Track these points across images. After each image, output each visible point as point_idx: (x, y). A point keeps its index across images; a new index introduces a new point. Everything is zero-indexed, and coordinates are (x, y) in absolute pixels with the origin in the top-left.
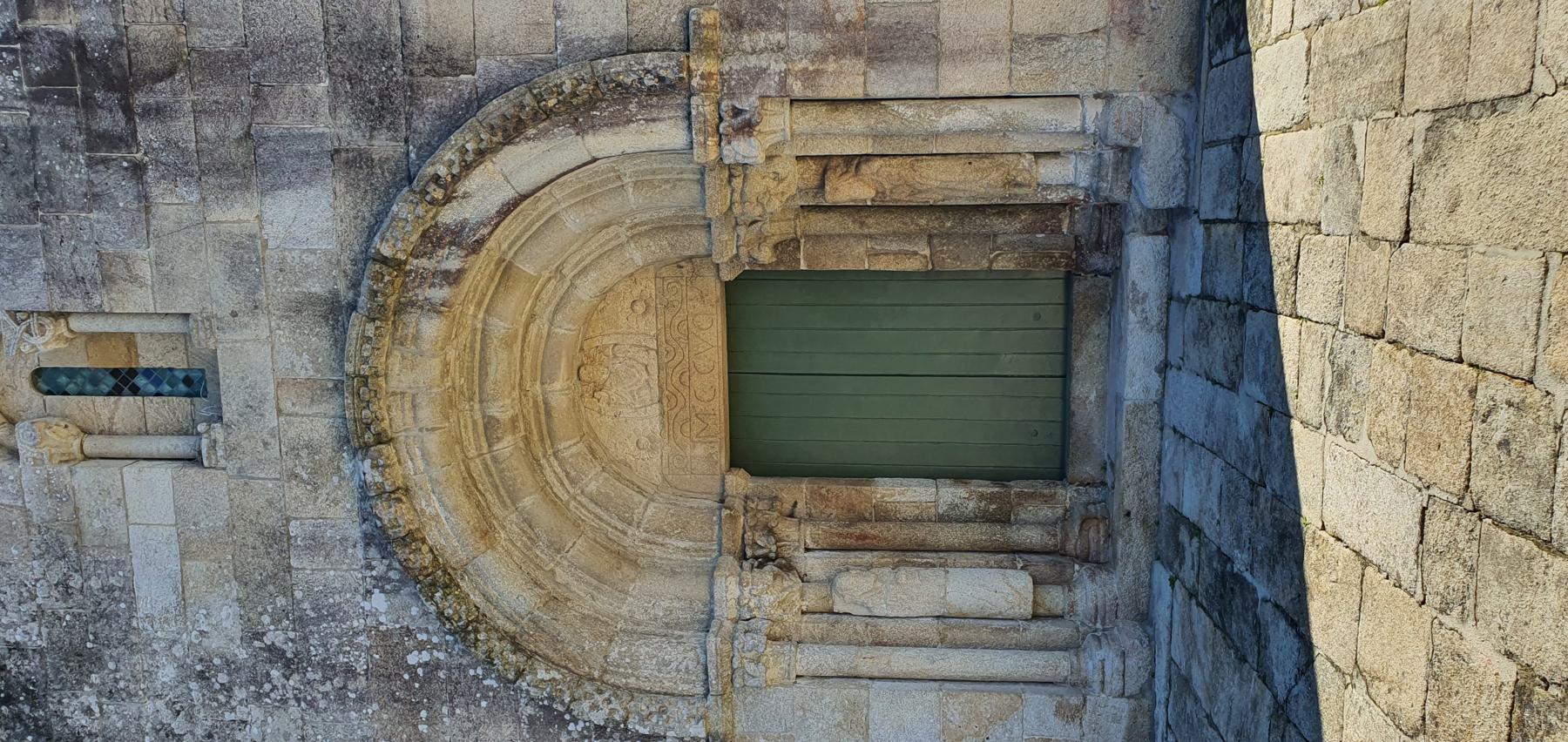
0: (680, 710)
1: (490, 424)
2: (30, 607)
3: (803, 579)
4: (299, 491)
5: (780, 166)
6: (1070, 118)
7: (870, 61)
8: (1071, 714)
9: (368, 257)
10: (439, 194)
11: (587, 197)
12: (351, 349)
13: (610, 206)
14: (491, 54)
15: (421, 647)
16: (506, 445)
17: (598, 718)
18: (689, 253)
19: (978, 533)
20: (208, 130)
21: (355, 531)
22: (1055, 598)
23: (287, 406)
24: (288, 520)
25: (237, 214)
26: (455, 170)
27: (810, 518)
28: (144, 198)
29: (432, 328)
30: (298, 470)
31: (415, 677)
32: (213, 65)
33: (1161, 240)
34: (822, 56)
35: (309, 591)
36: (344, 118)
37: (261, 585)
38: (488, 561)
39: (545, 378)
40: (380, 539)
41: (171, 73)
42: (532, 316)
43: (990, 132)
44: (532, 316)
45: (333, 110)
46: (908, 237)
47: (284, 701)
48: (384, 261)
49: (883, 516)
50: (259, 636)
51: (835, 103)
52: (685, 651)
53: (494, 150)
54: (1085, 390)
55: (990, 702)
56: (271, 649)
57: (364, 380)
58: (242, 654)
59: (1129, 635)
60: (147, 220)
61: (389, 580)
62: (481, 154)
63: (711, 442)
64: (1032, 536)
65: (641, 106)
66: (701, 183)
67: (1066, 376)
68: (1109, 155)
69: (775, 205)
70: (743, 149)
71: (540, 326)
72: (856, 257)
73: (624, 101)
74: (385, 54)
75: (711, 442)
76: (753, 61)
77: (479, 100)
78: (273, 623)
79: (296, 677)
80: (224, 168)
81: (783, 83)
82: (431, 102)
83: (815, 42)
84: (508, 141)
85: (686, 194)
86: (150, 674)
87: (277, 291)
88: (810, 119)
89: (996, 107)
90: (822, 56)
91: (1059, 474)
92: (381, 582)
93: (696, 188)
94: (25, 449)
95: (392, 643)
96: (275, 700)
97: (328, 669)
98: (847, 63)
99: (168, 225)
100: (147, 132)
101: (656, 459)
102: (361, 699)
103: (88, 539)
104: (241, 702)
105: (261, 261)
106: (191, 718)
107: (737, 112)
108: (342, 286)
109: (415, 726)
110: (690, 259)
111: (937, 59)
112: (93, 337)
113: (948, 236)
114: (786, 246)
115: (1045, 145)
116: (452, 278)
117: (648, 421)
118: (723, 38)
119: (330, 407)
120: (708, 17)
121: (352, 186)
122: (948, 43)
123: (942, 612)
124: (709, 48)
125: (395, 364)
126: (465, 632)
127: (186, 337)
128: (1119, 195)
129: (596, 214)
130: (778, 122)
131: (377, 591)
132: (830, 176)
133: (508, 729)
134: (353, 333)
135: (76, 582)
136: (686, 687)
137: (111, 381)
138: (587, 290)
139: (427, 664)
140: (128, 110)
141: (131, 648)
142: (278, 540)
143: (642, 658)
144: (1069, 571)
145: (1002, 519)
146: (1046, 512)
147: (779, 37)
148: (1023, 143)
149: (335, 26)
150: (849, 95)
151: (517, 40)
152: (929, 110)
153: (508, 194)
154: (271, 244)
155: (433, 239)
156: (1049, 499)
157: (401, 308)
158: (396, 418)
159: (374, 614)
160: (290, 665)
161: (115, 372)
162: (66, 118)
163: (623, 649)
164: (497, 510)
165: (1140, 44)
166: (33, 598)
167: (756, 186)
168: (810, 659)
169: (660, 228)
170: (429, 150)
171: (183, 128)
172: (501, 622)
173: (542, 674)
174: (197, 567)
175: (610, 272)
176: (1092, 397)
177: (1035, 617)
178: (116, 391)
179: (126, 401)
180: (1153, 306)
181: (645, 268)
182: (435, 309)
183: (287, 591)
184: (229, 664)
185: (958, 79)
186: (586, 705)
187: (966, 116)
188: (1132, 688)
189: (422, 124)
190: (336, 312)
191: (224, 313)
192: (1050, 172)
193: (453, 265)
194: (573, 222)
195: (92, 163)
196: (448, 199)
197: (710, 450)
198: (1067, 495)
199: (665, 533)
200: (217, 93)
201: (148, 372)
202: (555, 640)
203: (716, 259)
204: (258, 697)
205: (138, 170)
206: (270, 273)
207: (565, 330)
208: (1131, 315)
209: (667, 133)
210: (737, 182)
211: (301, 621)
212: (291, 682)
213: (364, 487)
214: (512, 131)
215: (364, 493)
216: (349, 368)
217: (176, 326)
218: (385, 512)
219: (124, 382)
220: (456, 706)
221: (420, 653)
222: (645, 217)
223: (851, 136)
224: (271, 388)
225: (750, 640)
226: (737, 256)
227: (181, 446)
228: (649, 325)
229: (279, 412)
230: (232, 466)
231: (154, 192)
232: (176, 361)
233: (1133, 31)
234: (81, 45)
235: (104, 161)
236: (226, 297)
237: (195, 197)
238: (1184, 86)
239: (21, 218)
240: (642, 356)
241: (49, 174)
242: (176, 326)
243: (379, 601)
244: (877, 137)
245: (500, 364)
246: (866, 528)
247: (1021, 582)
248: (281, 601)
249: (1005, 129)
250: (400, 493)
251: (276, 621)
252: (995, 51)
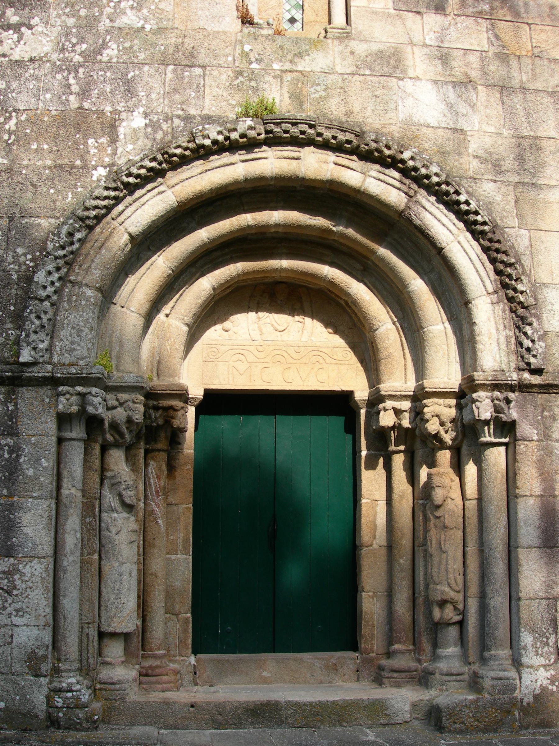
15: (101, 148)
17: (40, 277)
23: (288, 77)
24: (204, 67)
26: (464, 207)
30: (241, 78)
52: (88, 349)
56: (105, 45)
60: (412, 11)
61: (155, 131)
63: (228, 378)
65: (507, 337)
75: (228, 378)
78: (125, 48)
79: (81, 60)
92: (155, 126)
96: (63, 44)
99: (409, 24)
104: (64, 21)
109: (37, 140)
131: (147, 121)
136: (58, 349)
139: (88, 152)
143: (85, 314)
144: (134, 661)
154: (400, 83)
163: (92, 300)
172: (120, 207)
176: (265, 674)
177: (102, 635)
204: (67, 35)
212: (77, 56)
220: (51, 171)
221: (96, 147)
224: (300, 68)
229: (283, 71)
248: (142, 56)
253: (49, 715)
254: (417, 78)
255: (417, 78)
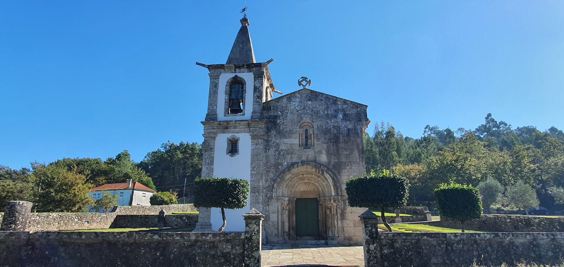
0: (275, 194)
1: (304, 175)
2: (284, 128)
3: (286, 207)
4: (297, 156)
5: (330, 204)
6: (336, 233)
7: (341, 213)
8: (275, 235)
9: (321, 165)
10: (327, 172)
11: (326, 185)
12: (312, 163)
13: (326, 187)
14: (340, 177)
15: (281, 167)
16: (301, 176)
17: (275, 186)
18: (321, 195)
19: (291, 226)
20: (332, 150)
21: (293, 161)
22: (286, 234)
23: (305, 155)
24: (294, 155)
25: (324, 152)
27: (292, 207)
28: (325, 143)
29: (314, 170)
31: (278, 167)
32: (338, 151)
33: (324, 243)
34: (341, 209)
35: (287, 156)
36: (333, 163)
37: (287, 152)
38: (291, 175)
39: (308, 179)
40: (293, 165)
41: (337, 147)
42: (314, 178)
43: (334, 225)
44: (314, 178)
45: (334, 162)
46: (323, 218)
47: (275, 153)
48: (321, 167)
49: (293, 215)
50: (282, 151)
51: (337, 210)
53: (331, 177)
54: (307, 237)
55: (276, 227)
56: (281, 152)
57: (309, 164)
58: (280, 149)
59: (283, 241)
62: (331, 176)
64: (291, 232)
65: (336, 191)
66: (328, 197)
67: (307, 236)
68: (332, 238)
69: (327, 204)
70: (332, 201)
71: (313, 179)
72: (320, 212)
73: (336, 190)
74: (340, 167)
76: (340, 202)
77: (336, 176)
80: (328, 151)
81: (338, 205)
82: (335, 171)
83: (342, 208)
84: (332, 179)
85: (327, 195)
86: (277, 140)
87: (317, 155)
88: (335, 207)
89: (337, 226)
90: (341, 209)
91: (296, 236)
92: (288, 164)
93: (328, 196)
94: (301, 129)
95: (281, 164)
97: (278, 158)
98: (341, 211)
99: (323, 145)
100: (331, 144)
101: (297, 190)
102: (275, 161)
103: (291, 135)
105: (320, 154)
106: (273, 143)
107: (336, 200)
108: (317, 161)
110: (320, 195)
111: (341, 220)
112: (311, 135)
113: (323, 222)
114: (321, 205)
115: (333, 231)
116: (319, 172)
117: (302, 190)
118: (342, 199)
119: (306, 160)
120: (344, 198)
121: (327, 163)
122: (342, 221)
123: (284, 222)
124: (341, 198)
125: (311, 167)
126: (284, 172)
127: (311, 146)
128: (328, 239)
129: (325, 186)
130: (335, 204)
132: (329, 210)
133: (272, 176)
134: (313, 163)
135: (287, 133)
137: (306, 136)
138: (317, 184)
140: (333, 142)
141: (280, 138)
142: (292, 154)
145: (292, 229)
146: (293, 234)
147: (343, 204)
148: (333, 229)
149: (342, 162)
150: (338, 211)
151: (341, 180)
152: (336, 219)
153: (327, 178)
155: (323, 171)
156: (294, 234)
157: (316, 167)
158: (305, 166)
159: (285, 163)
160: (279, 154)
161: (307, 137)
162: (332, 136)
164: (294, 175)
165: (343, 240)
166: (285, 129)
167: (329, 202)
168: (280, 207)
169: (323, 191)
170: (331, 171)
171: (332, 147)
172: (284, 176)
173: (279, 180)
174: (289, 145)
175: (319, 187)
178: (305, 137)
179: (305, 138)
180: (318, 243)
181: (319, 190)
182: (316, 170)
183: (286, 154)
184: (279, 148)
185: (339, 222)
186: (276, 184)
187: (336, 223)
188: (279, 242)
189: (333, 170)
190: (315, 161)
191: (315, 150)
192: (330, 232)
193: (320, 173)
194: (324, 184)
195: (328, 138)
196: (326, 173)
197: (298, 196)
198: (295, 236)
199: (291, 191)
200: (335, 151)
201: (307, 140)
202: (282, 181)
203: (320, 198)
204: (275, 150)
205: (328, 143)
206: (319, 155)
207: (312, 182)
208: (316, 241)
209: (333, 194)
210: (329, 200)
211: (283, 155)
213: (299, 163)
214: (333, 179)
215: (297, 163)
216: (310, 162)
217: (313, 144)
218: (296, 165)
219: (306, 138)
222: (324, 191)
223: (334, 212)
225: (283, 201)
226: (320, 200)
227: (301, 144)
228: (312, 190)
230: (299, 149)
231: (326, 144)
232: (309, 143)
233: (344, 239)
234: (339, 139)
235: (328, 140)
236: (316, 150)
237: (325, 148)
238: (340, 244)
239: (323, 131)
240: (309, 189)
241: (327, 135)
242: (313, 144)
243: (286, 163)
244: (334, 214)
245: (310, 176)
246: (291, 214)
247: (287, 230)
249: (335, 227)
250: (298, 167)
251: (283, 153)
252: (342, 225)
253: (277, 242)
254: (324, 154)
255: (324, 154)
